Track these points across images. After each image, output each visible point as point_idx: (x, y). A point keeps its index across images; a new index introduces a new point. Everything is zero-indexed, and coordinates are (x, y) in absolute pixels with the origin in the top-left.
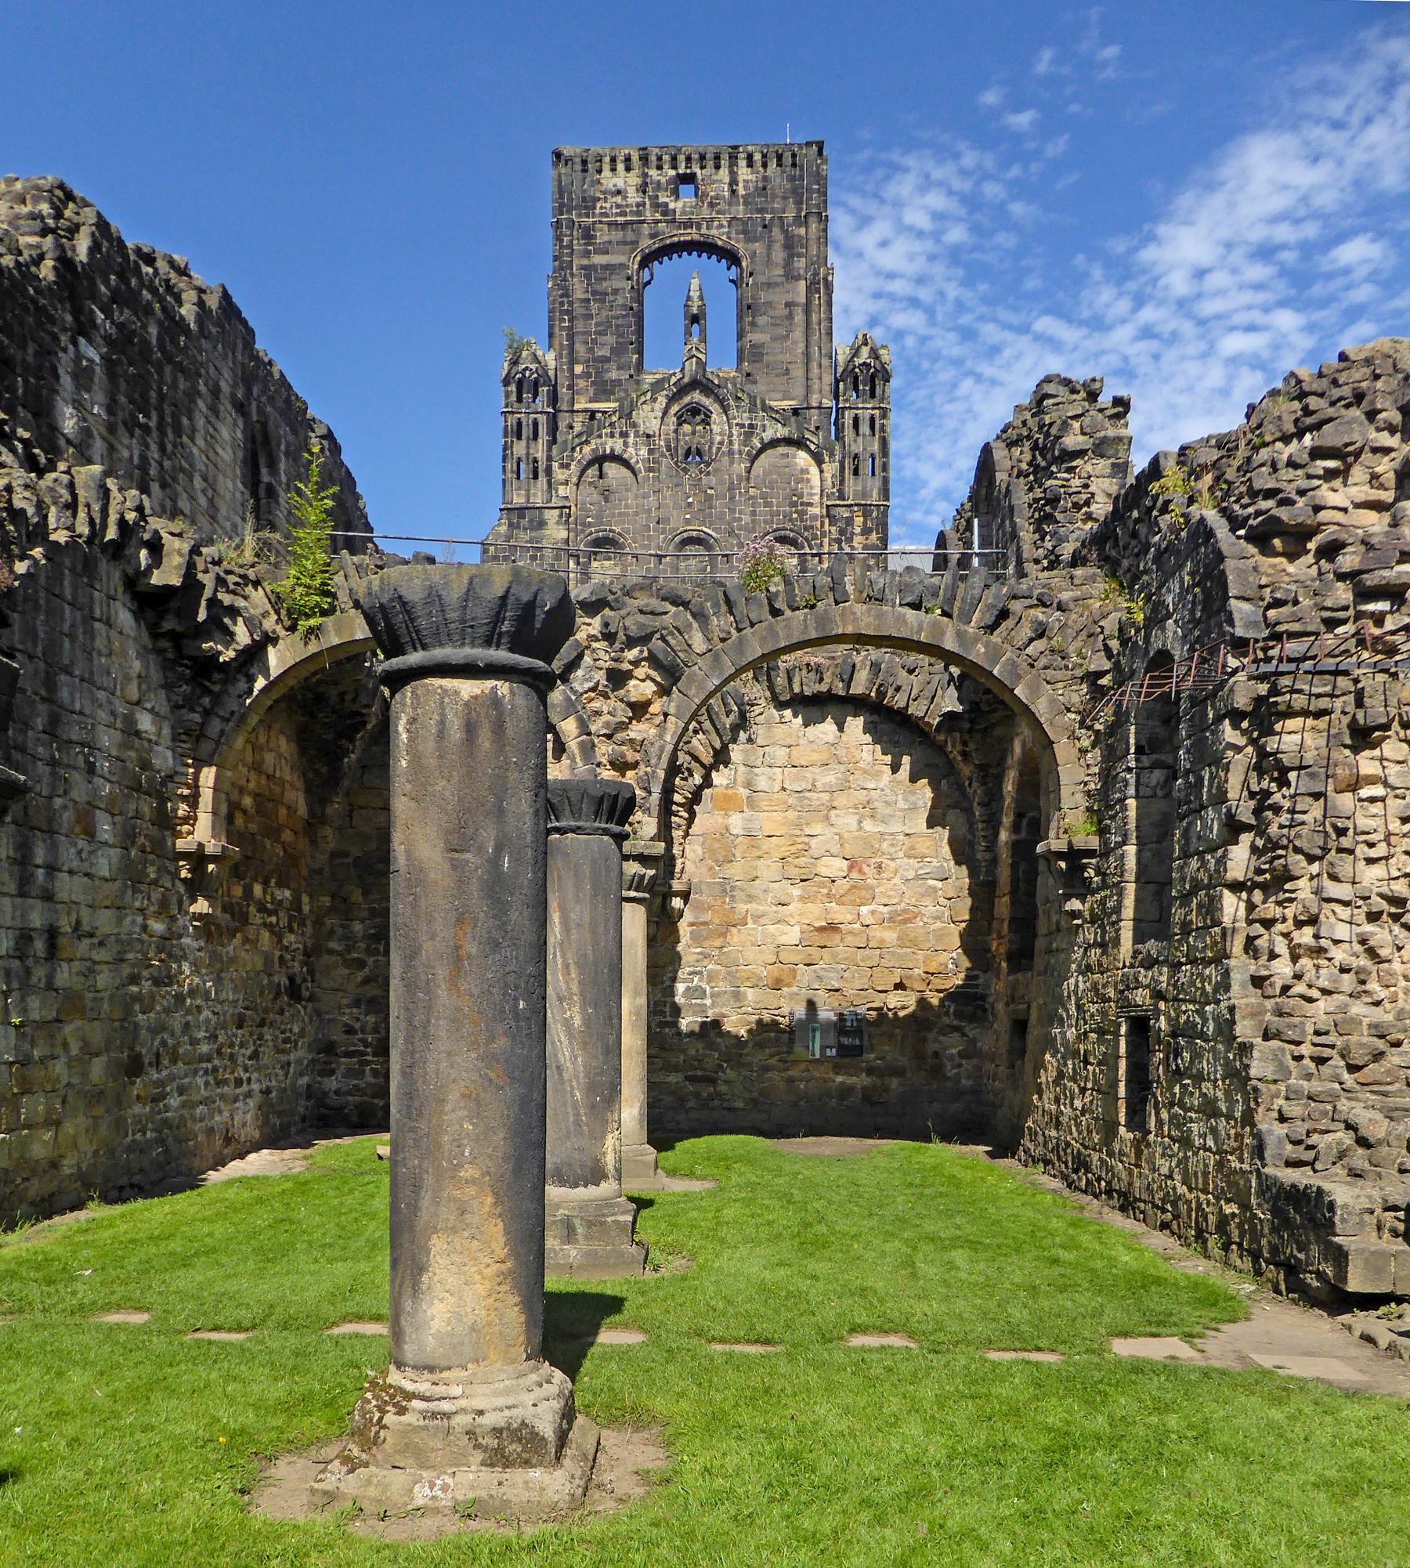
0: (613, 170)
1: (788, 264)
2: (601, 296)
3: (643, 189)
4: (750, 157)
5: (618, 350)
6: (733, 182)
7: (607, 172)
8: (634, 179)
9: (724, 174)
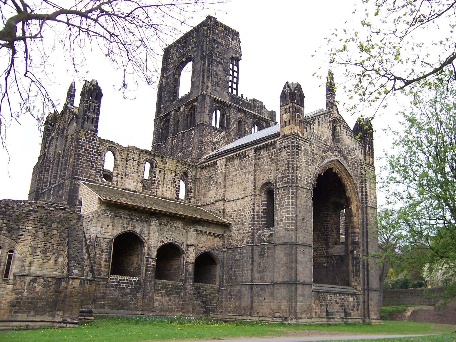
5: (169, 98)
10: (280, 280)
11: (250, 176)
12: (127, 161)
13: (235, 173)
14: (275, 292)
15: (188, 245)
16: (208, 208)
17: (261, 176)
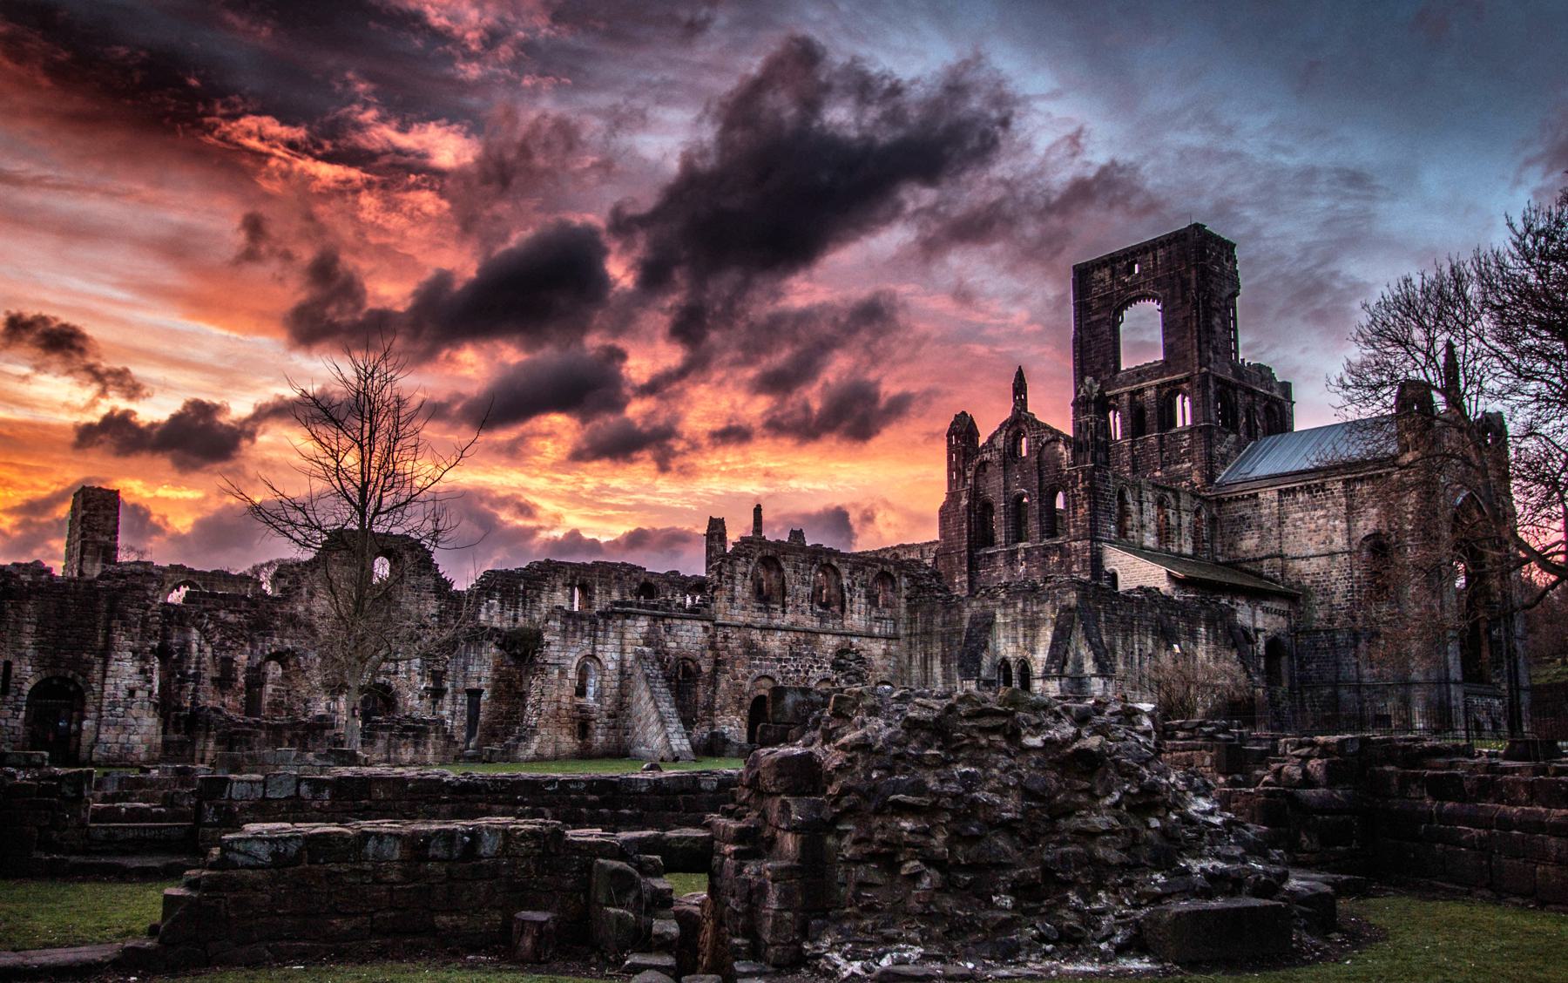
1: (1183, 295)
2: (1095, 337)
3: (1112, 276)
5: (1105, 365)
6: (1155, 258)
8: (1107, 272)
15: (1257, 631)
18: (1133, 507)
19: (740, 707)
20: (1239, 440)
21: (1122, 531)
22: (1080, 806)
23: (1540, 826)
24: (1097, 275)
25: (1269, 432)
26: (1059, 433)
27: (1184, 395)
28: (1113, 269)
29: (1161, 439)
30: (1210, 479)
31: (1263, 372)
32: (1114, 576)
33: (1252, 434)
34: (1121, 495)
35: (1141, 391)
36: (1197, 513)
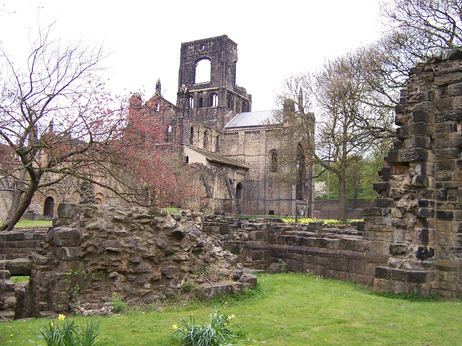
0: (190, 46)
3: (195, 49)
4: (213, 39)
7: (189, 46)
9: (208, 43)
10: (284, 198)
11: (263, 145)
12: (199, 133)
13: (251, 141)
14: (280, 203)
15: (234, 180)
16: (232, 158)
17: (270, 146)
18: (196, 134)
19: (41, 201)
20: (233, 112)
21: (191, 142)
22: (176, 251)
23: (317, 253)
24: (189, 48)
25: (243, 112)
26: (171, 104)
27: (216, 95)
28: (195, 46)
29: (207, 109)
30: (223, 125)
31: (242, 91)
32: (187, 158)
33: (238, 112)
34: (192, 129)
35: (202, 92)
36: (217, 137)
